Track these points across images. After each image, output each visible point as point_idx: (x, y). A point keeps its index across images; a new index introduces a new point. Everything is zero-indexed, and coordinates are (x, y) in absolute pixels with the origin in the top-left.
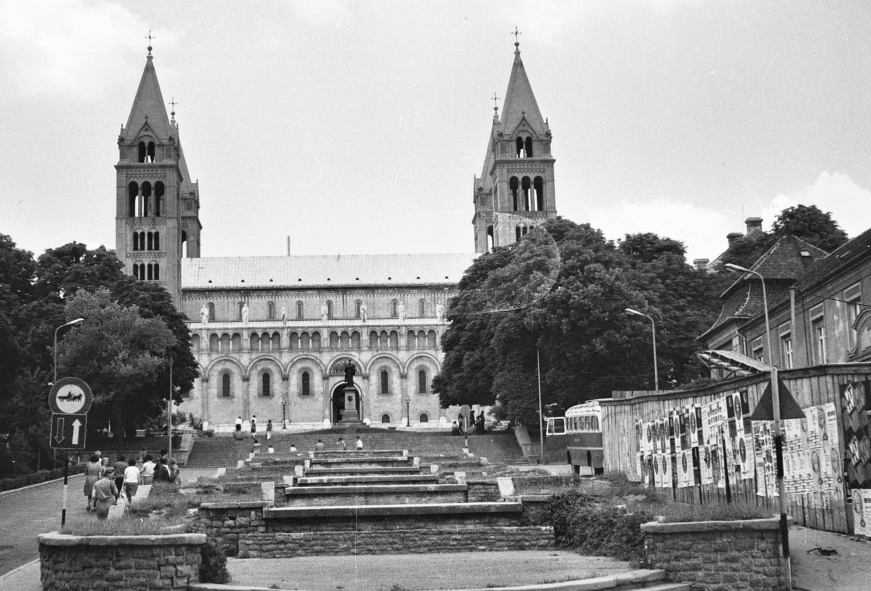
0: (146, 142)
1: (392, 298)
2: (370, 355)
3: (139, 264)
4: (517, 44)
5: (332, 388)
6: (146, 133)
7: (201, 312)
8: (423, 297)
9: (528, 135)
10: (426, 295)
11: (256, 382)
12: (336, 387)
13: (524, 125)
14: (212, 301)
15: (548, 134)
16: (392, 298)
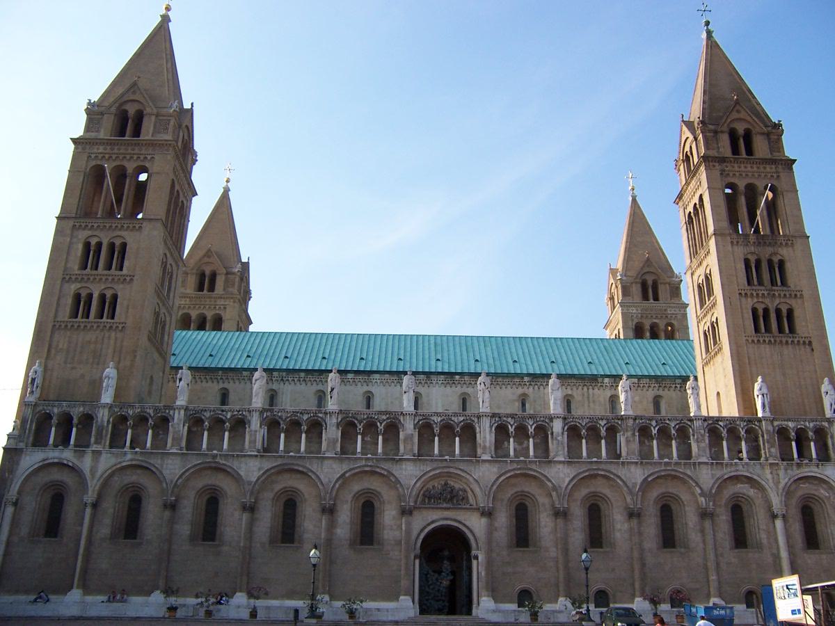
0: (132, 110)
1: (520, 391)
2: (495, 470)
3: (84, 294)
4: (707, 23)
5: (419, 535)
6: (132, 98)
7: (179, 376)
8: (570, 393)
9: (746, 126)
10: (575, 388)
11: (269, 515)
12: (426, 531)
13: (738, 111)
14: (226, 385)
15: (778, 126)
16: (520, 391)
